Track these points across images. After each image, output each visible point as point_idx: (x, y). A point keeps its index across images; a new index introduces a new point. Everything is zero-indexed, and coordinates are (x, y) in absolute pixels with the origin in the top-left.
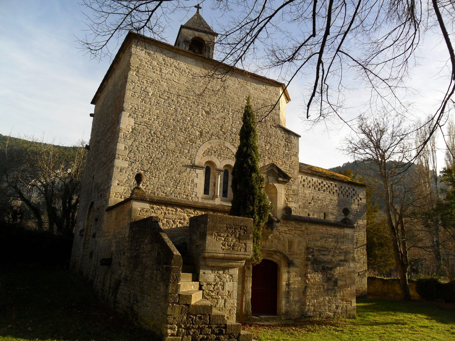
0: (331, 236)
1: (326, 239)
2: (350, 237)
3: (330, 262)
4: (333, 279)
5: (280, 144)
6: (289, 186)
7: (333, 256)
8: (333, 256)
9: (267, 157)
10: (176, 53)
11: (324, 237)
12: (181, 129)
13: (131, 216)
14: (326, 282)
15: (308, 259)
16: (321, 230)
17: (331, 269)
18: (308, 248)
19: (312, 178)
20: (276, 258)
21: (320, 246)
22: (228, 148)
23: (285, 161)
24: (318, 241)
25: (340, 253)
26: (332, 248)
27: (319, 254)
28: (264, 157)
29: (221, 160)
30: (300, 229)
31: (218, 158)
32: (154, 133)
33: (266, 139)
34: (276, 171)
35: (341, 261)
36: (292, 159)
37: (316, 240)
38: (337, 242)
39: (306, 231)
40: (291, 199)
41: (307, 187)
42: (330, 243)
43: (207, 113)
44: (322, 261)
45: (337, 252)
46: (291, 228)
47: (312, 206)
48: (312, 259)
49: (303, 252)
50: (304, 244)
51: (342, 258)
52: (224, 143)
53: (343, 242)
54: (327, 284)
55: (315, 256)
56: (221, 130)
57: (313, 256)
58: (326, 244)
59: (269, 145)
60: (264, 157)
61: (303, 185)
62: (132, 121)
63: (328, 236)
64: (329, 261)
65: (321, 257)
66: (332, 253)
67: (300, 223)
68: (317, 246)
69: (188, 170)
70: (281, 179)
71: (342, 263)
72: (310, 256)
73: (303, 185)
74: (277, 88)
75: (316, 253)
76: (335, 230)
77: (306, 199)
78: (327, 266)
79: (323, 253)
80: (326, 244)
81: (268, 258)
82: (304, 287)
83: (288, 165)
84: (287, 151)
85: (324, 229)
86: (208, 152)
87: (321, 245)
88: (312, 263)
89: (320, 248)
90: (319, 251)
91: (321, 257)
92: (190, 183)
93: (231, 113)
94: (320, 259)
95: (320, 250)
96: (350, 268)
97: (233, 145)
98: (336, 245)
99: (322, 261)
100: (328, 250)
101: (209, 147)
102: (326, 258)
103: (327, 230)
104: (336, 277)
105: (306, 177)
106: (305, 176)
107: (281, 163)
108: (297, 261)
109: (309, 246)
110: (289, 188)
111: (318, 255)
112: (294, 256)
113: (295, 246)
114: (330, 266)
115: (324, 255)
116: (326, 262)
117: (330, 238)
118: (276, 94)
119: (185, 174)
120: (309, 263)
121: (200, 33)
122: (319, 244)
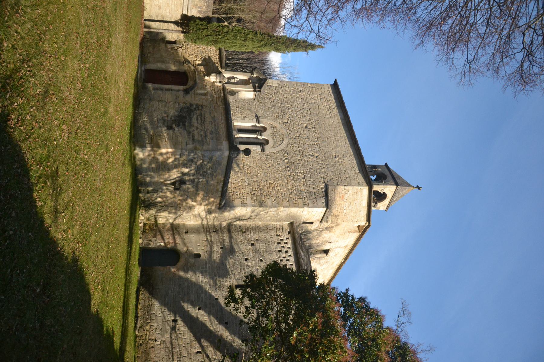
0: (216, 127)
1: (213, 122)
2: (219, 147)
3: (191, 125)
4: (174, 126)
5: (309, 187)
6: (268, 196)
7: (197, 128)
8: (197, 128)
9: (289, 173)
10: (341, 107)
11: (215, 121)
12: (284, 110)
13: (208, 20)
14: (171, 118)
15: (191, 105)
16: (220, 118)
17: (184, 125)
18: (202, 106)
19: (294, 264)
20: (190, 83)
21: (205, 117)
22: (283, 141)
23: (293, 192)
24: (210, 115)
25: (201, 135)
26: (205, 128)
27: (198, 115)
28: (288, 171)
29: (270, 135)
30: (218, 101)
31: (271, 133)
32: (273, 96)
33: (307, 173)
34: (262, 82)
35: (193, 136)
36: (299, 200)
37: (210, 113)
38: (212, 133)
39: (216, 105)
40: (255, 198)
41: (280, 257)
42: (209, 127)
43: (306, 127)
44: (191, 117)
45: (202, 133)
46: (217, 94)
47: (258, 263)
48: (192, 108)
49: (198, 103)
50: (205, 103)
51: (196, 138)
52: (286, 138)
53: (212, 139)
54: (169, 119)
55: (195, 111)
56: (296, 136)
57: (195, 109)
58: (208, 122)
59: (303, 176)
60: (288, 171)
61: (280, 251)
62: (277, 85)
63: (216, 125)
64: (192, 124)
65: (195, 116)
66: (199, 126)
67: (223, 101)
68: (204, 114)
69: (254, 115)
70: (257, 85)
71: (191, 136)
72: (194, 107)
73: (280, 251)
74: (365, 184)
75: (198, 112)
76: (223, 131)
77: (265, 253)
78: (187, 121)
79: (199, 118)
80: (208, 122)
81: (189, 79)
82: (166, 101)
83: (291, 196)
84: (305, 194)
85: (223, 121)
86: (272, 126)
87: (207, 117)
88: (188, 108)
89: (203, 116)
90: (201, 115)
91: (195, 116)
92: (243, 115)
93: (316, 143)
94: (192, 115)
95: (202, 116)
96: (187, 145)
97: (288, 145)
98: (208, 131)
99: (191, 117)
100: (203, 122)
101: (278, 128)
102: (194, 120)
103: (222, 123)
104: (176, 129)
105: (292, 255)
106: (292, 252)
107: (289, 188)
108: (189, 98)
109: (204, 107)
110: (266, 196)
111: (196, 113)
112: (193, 96)
113: (203, 97)
114: (187, 124)
115: (197, 120)
116: (191, 120)
117: (215, 125)
118: (359, 182)
119: (249, 112)
120: (188, 105)
121: (390, 175)
122: (207, 115)
